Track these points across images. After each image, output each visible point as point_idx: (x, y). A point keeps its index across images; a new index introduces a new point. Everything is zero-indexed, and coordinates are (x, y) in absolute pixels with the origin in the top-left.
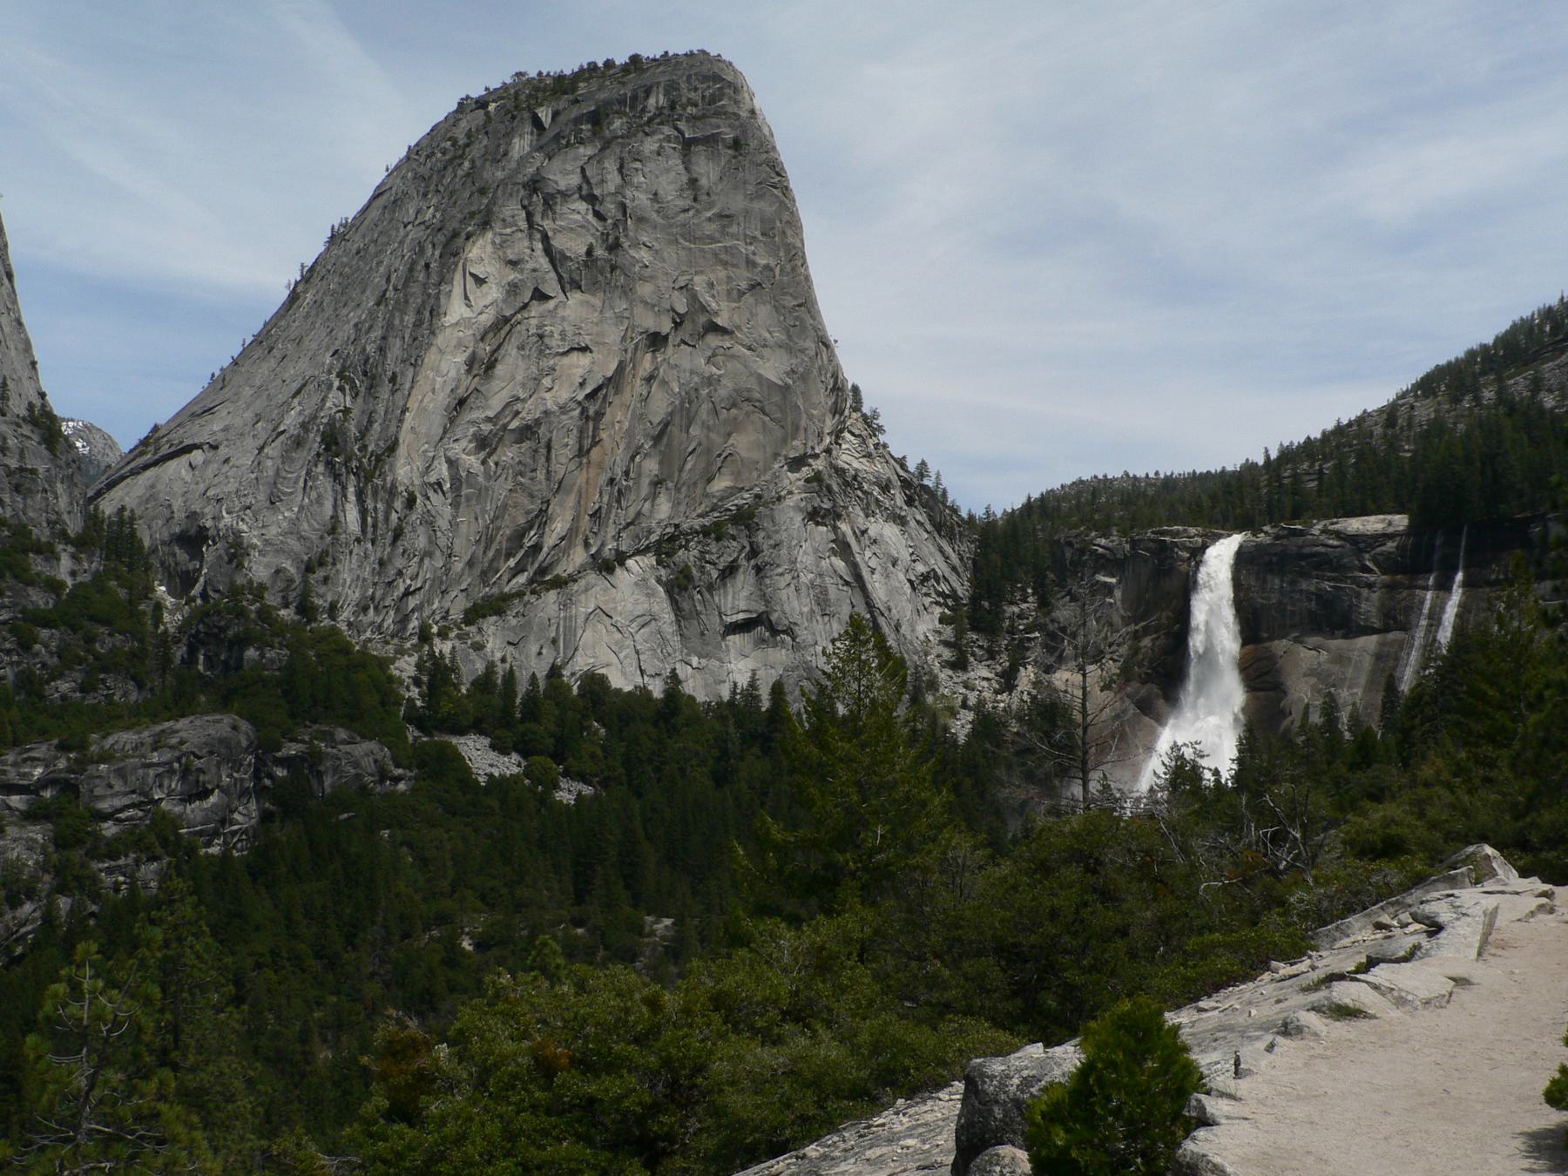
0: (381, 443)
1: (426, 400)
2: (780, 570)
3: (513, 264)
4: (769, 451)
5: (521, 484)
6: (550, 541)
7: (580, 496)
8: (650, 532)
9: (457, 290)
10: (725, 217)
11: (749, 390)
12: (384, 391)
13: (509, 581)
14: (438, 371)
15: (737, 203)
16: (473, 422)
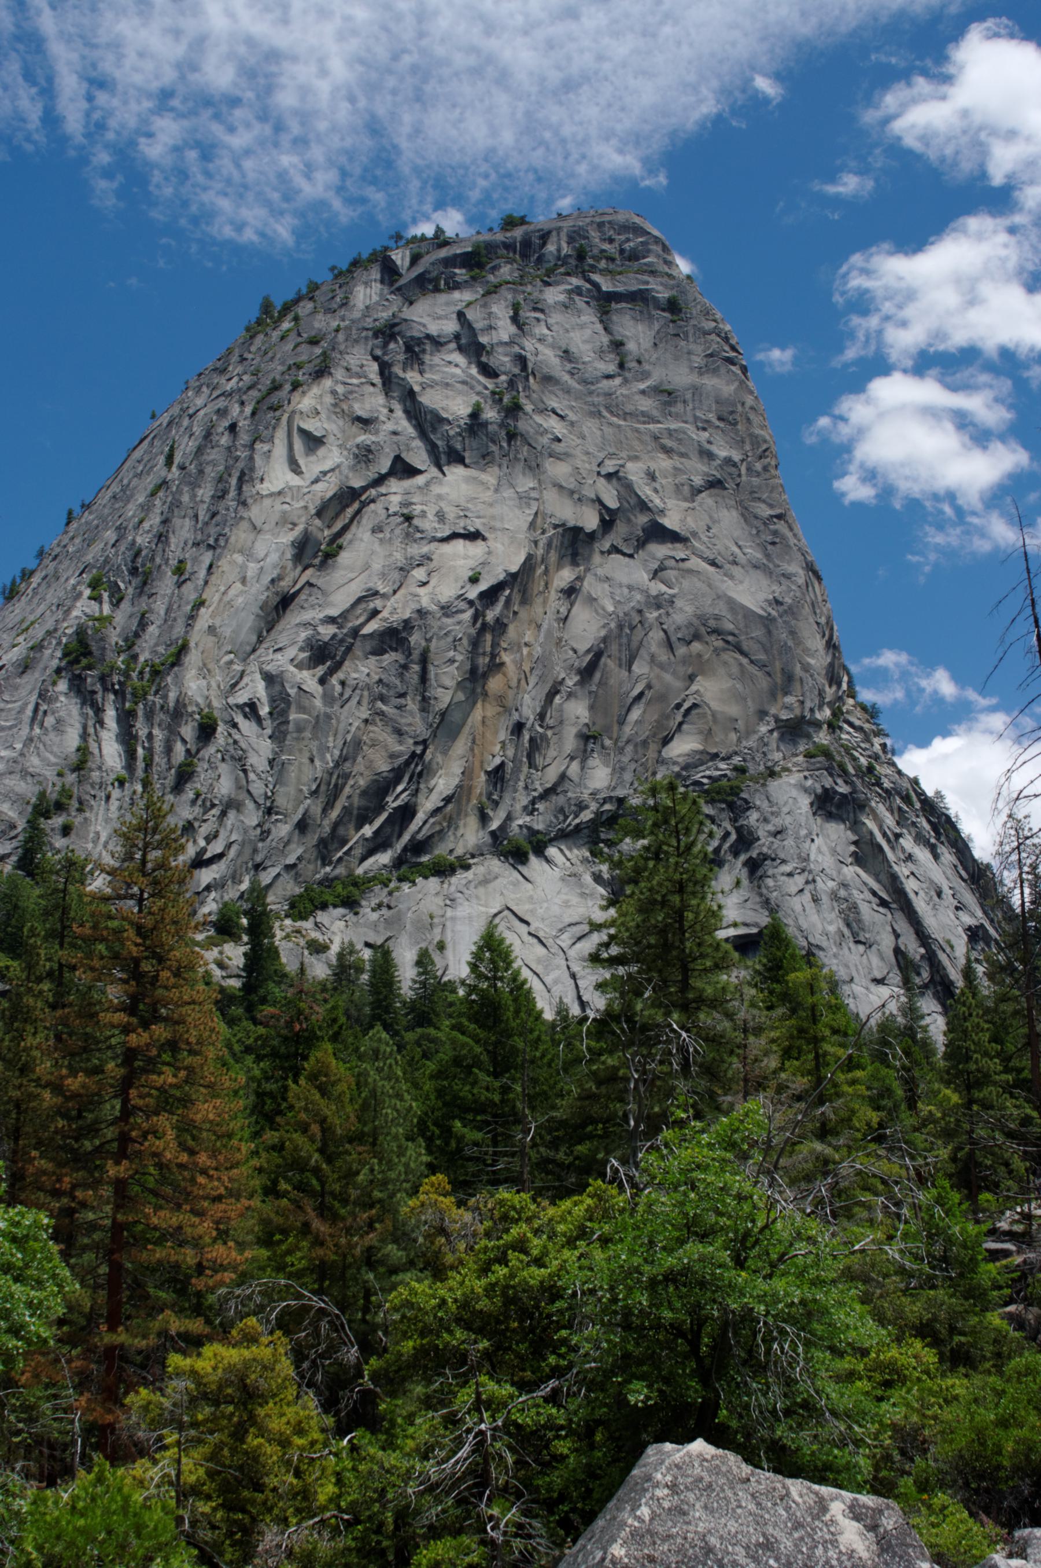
0: (161, 649)
1: (232, 592)
2: (787, 868)
4: (752, 706)
5: (382, 714)
6: (427, 804)
7: (474, 742)
8: (581, 807)
9: (280, 449)
10: (667, 395)
11: (717, 618)
12: (166, 585)
13: (363, 859)
14: (248, 553)
15: (680, 377)
16: (306, 625)
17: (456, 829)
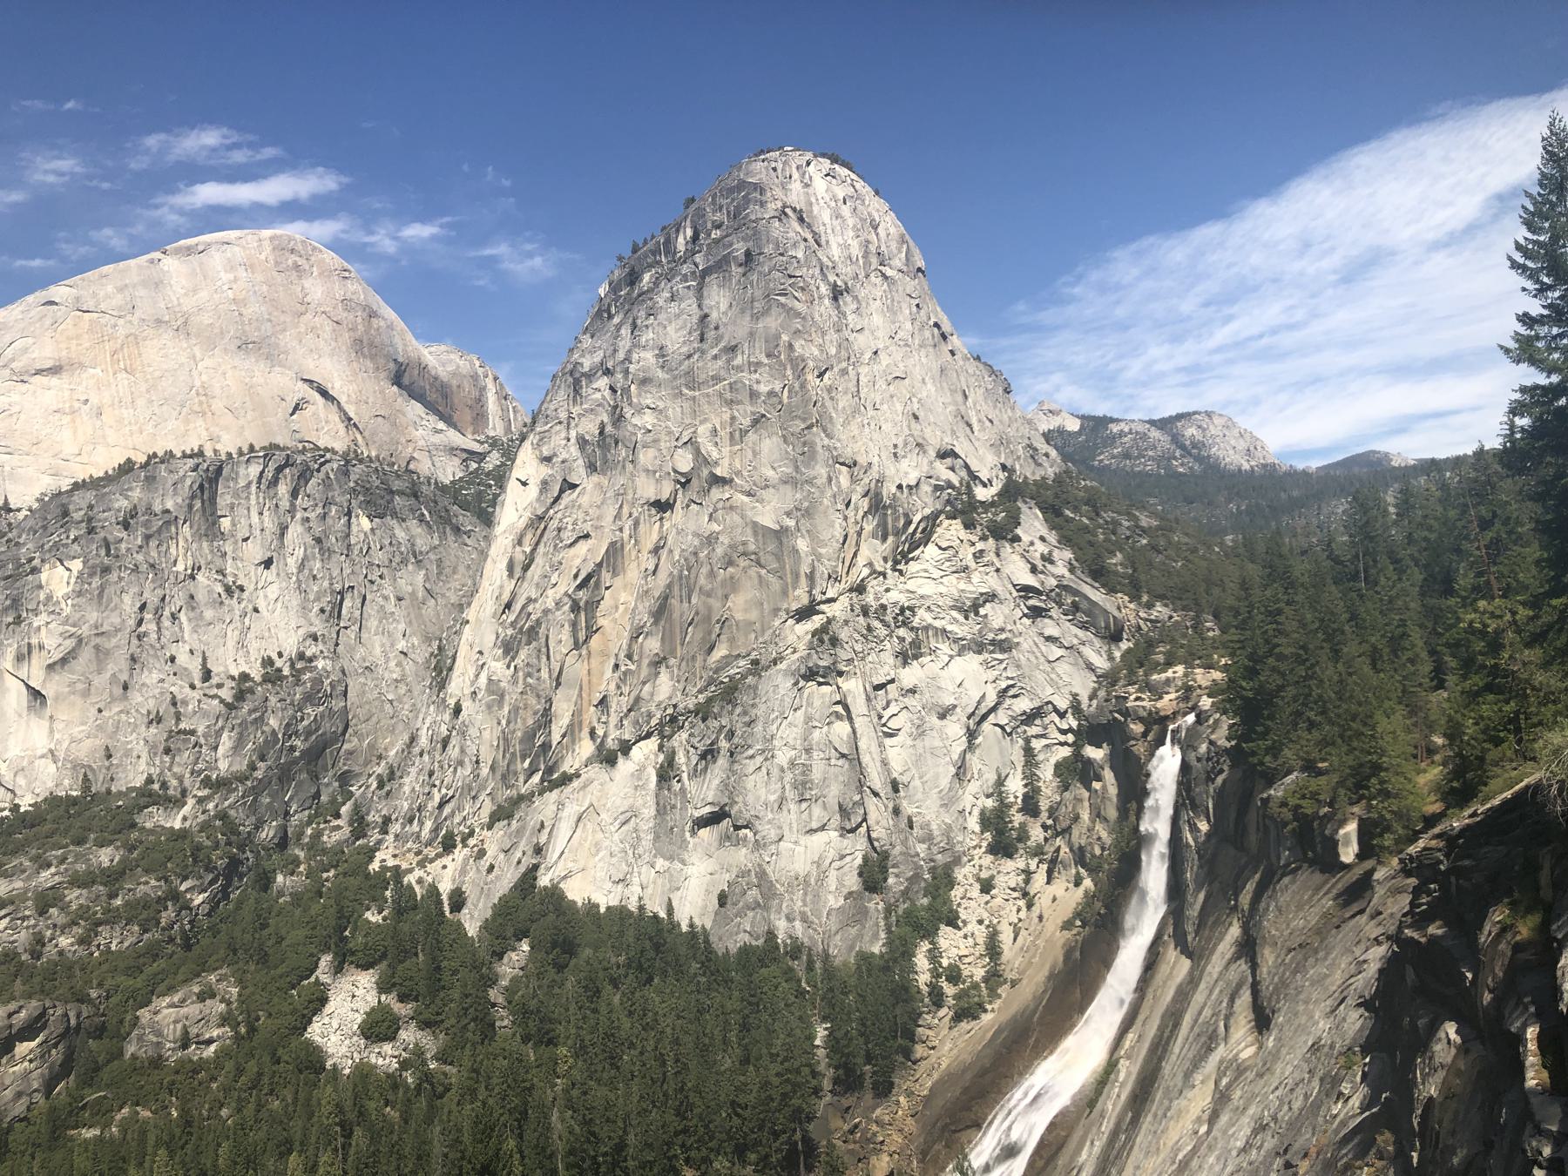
2: (750, 752)
3: (547, 459)
5: (530, 685)
6: (556, 737)
8: (650, 716)
11: (744, 543)
17: (573, 751)
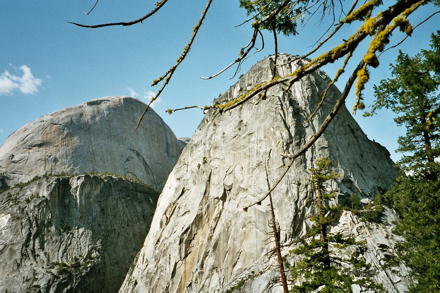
3: (179, 179)
4: (259, 247)
